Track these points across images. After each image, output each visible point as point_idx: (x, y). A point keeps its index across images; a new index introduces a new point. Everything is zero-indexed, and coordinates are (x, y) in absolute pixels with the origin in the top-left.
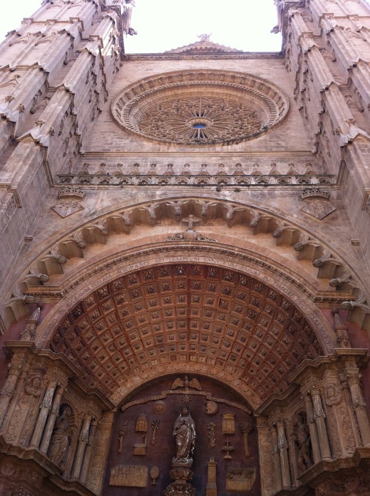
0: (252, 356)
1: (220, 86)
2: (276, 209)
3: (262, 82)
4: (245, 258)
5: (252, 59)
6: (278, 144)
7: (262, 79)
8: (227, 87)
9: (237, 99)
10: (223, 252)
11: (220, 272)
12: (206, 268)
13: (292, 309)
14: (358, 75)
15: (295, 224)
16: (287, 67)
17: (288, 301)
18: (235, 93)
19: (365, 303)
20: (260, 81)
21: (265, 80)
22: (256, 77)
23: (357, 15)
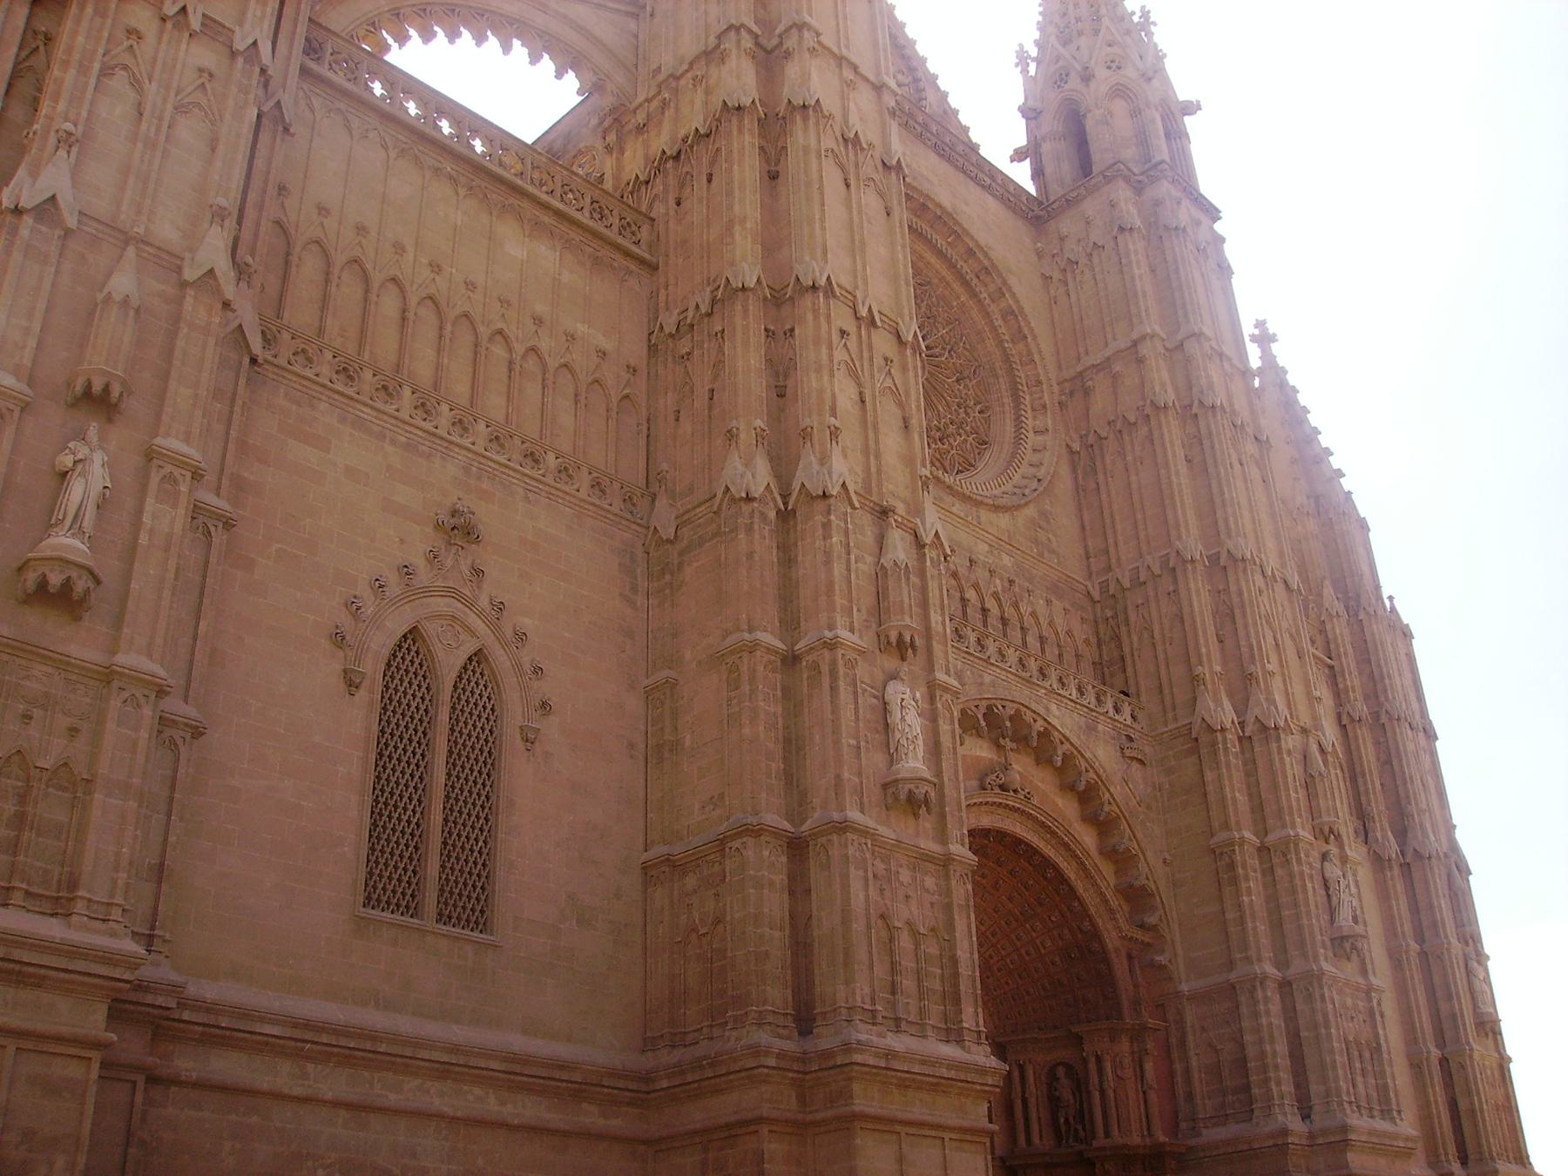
0: (995, 959)
1: (940, 254)
2: (1103, 768)
3: (1014, 307)
4: (1066, 846)
5: (994, 196)
6: (1049, 539)
7: (1017, 301)
8: (952, 266)
9: (955, 304)
10: (1042, 825)
11: (1032, 851)
12: (1018, 841)
13: (1096, 935)
14: (1243, 583)
15: (1118, 807)
16: (1047, 279)
17: (1093, 924)
18: (957, 286)
19: (1170, 961)
20: (1011, 302)
21: (1021, 309)
22: (1010, 289)
23: (1230, 359)
